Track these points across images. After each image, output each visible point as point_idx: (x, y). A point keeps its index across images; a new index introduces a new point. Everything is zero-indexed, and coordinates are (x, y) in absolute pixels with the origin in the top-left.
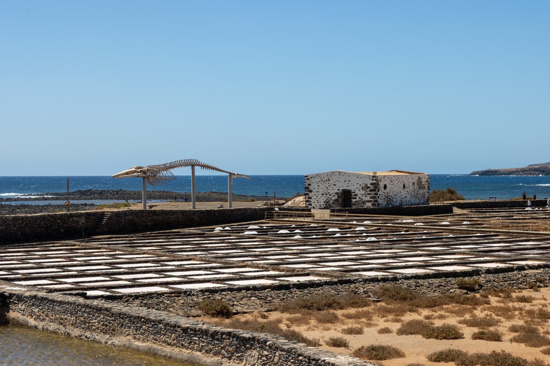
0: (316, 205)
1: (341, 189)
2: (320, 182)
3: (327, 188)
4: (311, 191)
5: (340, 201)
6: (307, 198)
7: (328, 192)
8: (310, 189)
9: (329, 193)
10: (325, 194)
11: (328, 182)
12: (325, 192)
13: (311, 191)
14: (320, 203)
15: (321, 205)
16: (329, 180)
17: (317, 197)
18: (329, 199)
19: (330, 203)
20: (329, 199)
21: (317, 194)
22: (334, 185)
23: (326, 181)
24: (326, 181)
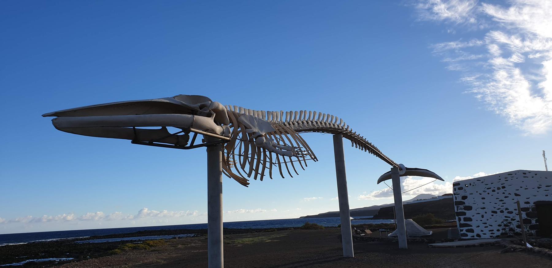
0: (482, 231)
1: (532, 201)
2: (484, 191)
3: (501, 201)
4: (469, 208)
5: (534, 222)
6: (462, 220)
7: (504, 207)
8: (467, 204)
9: (507, 209)
10: (498, 211)
11: (502, 190)
12: (499, 207)
13: (469, 208)
14: (491, 228)
15: (493, 230)
16: (504, 187)
17: (483, 216)
18: (509, 219)
19: (512, 226)
20: (509, 219)
21: (482, 212)
22: (516, 195)
23: (499, 189)
24: (499, 189)
